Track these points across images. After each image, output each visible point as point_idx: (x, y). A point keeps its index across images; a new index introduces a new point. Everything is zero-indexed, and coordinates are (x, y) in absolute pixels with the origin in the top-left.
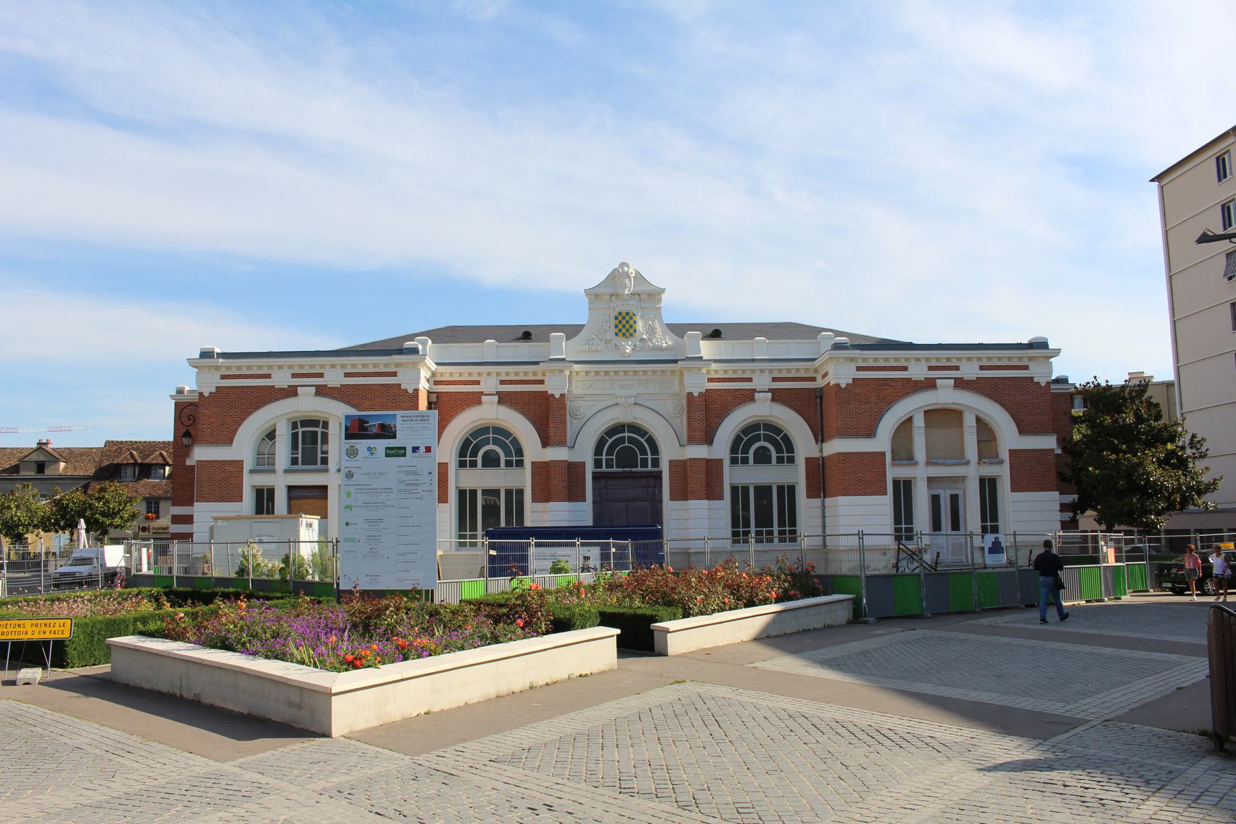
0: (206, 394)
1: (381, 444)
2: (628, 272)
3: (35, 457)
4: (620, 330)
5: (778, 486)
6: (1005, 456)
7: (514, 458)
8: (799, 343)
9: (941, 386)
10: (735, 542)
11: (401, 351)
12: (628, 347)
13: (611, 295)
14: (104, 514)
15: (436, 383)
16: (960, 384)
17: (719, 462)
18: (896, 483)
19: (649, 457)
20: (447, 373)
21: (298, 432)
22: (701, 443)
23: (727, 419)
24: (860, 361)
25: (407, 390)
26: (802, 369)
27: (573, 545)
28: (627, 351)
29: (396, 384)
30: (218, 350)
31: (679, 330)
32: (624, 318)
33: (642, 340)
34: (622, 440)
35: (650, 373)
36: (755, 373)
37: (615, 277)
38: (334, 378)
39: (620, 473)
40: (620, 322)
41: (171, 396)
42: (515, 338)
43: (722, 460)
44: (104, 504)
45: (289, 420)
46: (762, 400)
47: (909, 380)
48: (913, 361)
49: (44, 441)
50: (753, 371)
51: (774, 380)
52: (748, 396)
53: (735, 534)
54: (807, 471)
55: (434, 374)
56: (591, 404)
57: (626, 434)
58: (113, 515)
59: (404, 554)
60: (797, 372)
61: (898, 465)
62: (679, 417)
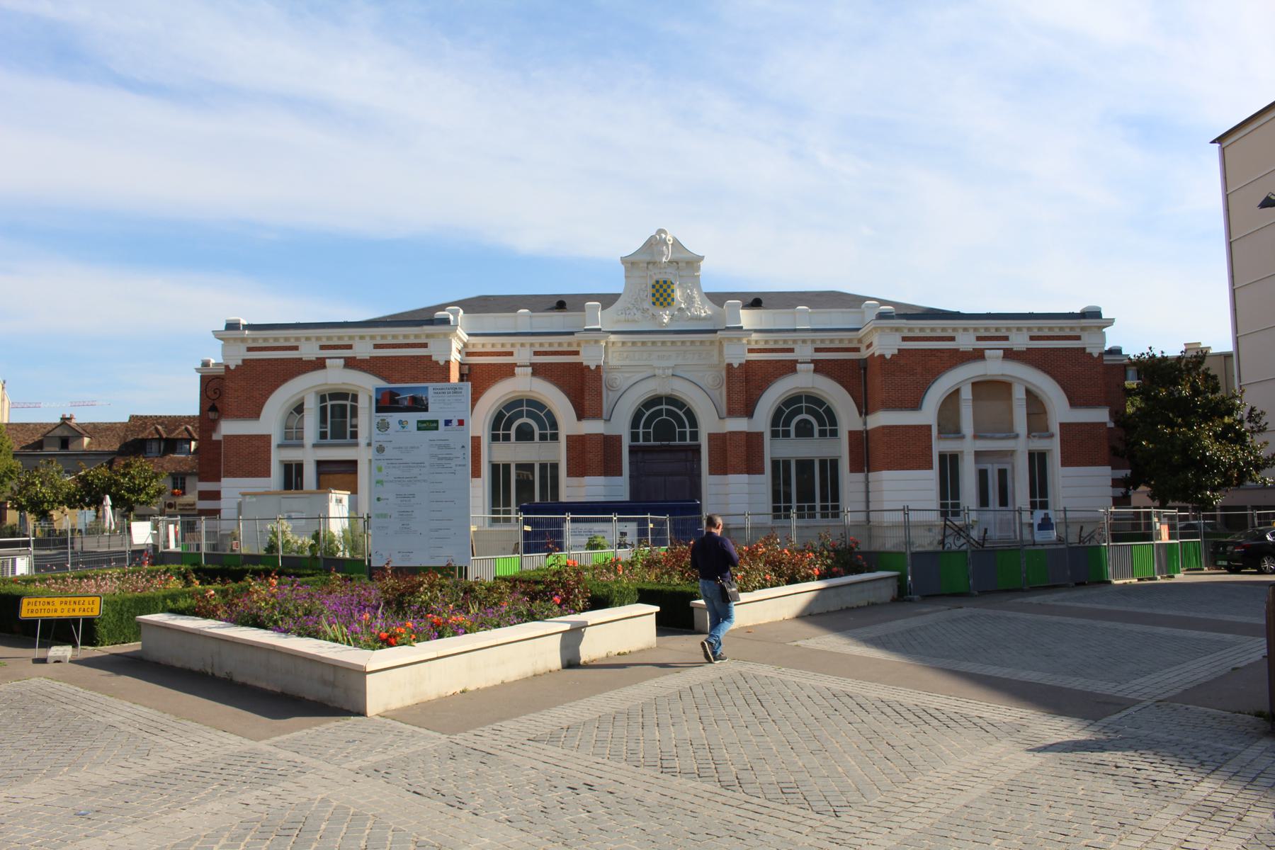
0: (232, 367)
1: (413, 418)
2: (665, 239)
3: (58, 432)
4: (658, 299)
6: (1055, 429)
7: (549, 432)
8: (842, 312)
9: (989, 358)
10: (776, 517)
11: (432, 322)
12: (666, 317)
13: (648, 263)
14: (129, 490)
15: (468, 354)
16: (1010, 355)
17: (760, 435)
18: (942, 457)
19: (688, 430)
20: (479, 343)
21: (326, 405)
22: (741, 416)
24: (906, 331)
27: (610, 520)
28: (665, 321)
30: (243, 322)
31: (718, 299)
32: (661, 286)
33: (680, 309)
34: (659, 412)
35: (688, 344)
37: (652, 244)
38: (363, 350)
39: (658, 446)
40: (658, 291)
41: (196, 369)
42: (549, 307)
44: (130, 480)
45: (317, 393)
47: (957, 350)
49: (68, 416)
50: (795, 341)
51: (817, 350)
52: (790, 368)
53: (776, 509)
54: (850, 444)
56: (627, 375)
57: (664, 407)
58: (139, 490)
59: (437, 530)
60: (840, 343)
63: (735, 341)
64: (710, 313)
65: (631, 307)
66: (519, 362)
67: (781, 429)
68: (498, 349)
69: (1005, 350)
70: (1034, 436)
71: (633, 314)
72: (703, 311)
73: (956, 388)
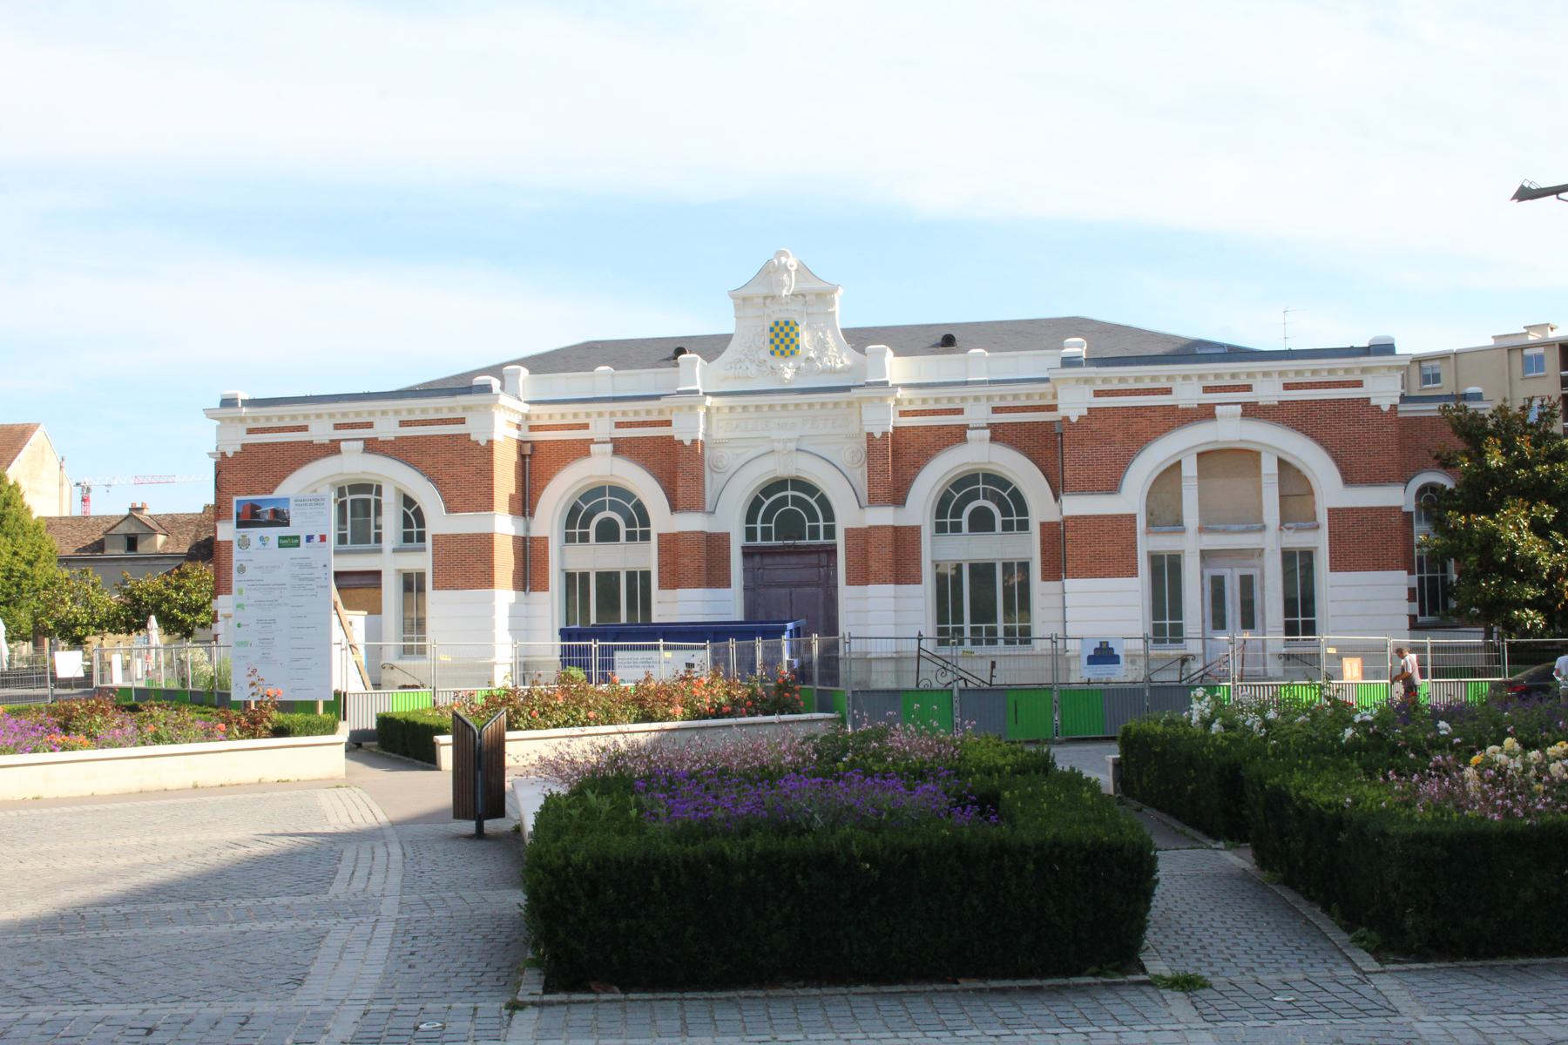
0: (230, 455)
1: (274, 533)
2: (786, 263)
3: (124, 529)
4: (777, 347)
6: (1323, 518)
7: (638, 529)
8: (1035, 355)
9: (1221, 416)
10: (942, 643)
11: (469, 390)
12: (788, 371)
13: (765, 298)
14: (183, 608)
15: (532, 428)
16: (1252, 411)
17: (916, 530)
18: (1156, 560)
19: (821, 524)
20: (544, 414)
21: (345, 501)
24: (1099, 382)
27: (656, 648)
29: (465, 435)
30: (243, 395)
31: (859, 338)
32: (782, 329)
33: (808, 359)
34: (783, 501)
37: (770, 272)
38: (387, 429)
39: (780, 547)
40: (777, 335)
41: (209, 454)
42: (666, 357)
44: (185, 594)
45: (333, 485)
47: (1174, 408)
49: (139, 505)
50: (963, 399)
52: (958, 435)
53: (941, 632)
54: (1043, 542)
55: (527, 417)
57: (789, 493)
58: (198, 610)
59: (298, 660)
60: (1040, 398)
61: (1158, 533)
67: (949, 520)
68: (570, 420)
69: (1244, 405)
70: (1289, 529)
72: (839, 361)
73: (1177, 459)
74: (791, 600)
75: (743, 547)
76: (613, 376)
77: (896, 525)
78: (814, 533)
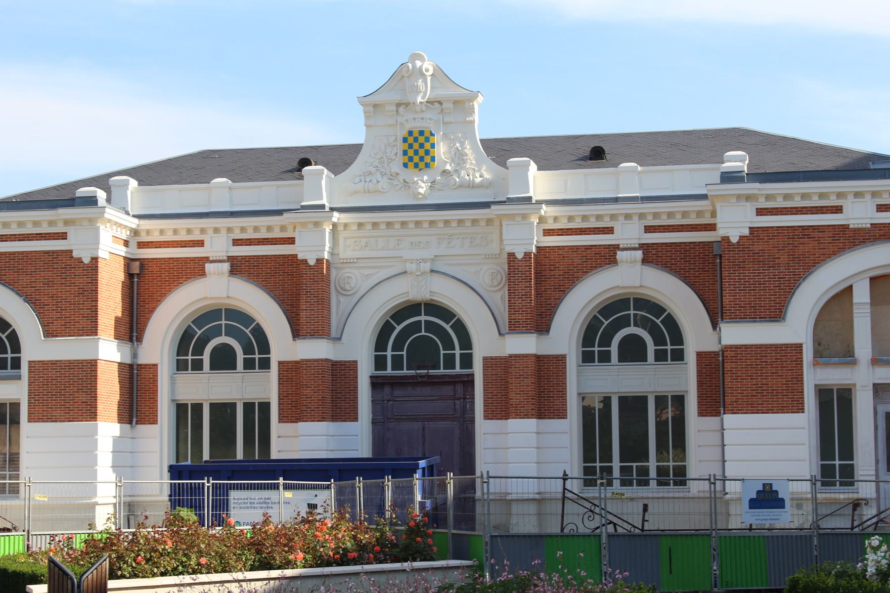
2: (421, 68)
4: (411, 159)
5: (620, 398)
8: (691, 170)
11: (72, 202)
12: (423, 185)
13: (398, 105)
15: (141, 245)
17: (560, 360)
18: (824, 394)
19: (458, 352)
20: (154, 229)
22: (528, 331)
23: (571, 294)
24: (762, 199)
25: (80, 258)
26: (678, 212)
27: (276, 487)
28: (421, 191)
29: (66, 251)
32: (416, 140)
35: (454, 224)
36: (617, 220)
37: (403, 76)
39: (412, 377)
40: (410, 146)
42: (290, 168)
43: (564, 357)
46: (627, 262)
47: (845, 227)
48: (851, 197)
50: (613, 217)
51: (649, 229)
53: (588, 471)
55: (135, 232)
56: (367, 272)
57: (423, 318)
61: (826, 364)
62: (500, 289)
63: (519, 219)
64: (488, 177)
65: (373, 170)
66: (212, 256)
68: (183, 237)
71: (374, 181)
72: (477, 175)
74: (424, 436)
75: (371, 377)
76: (230, 188)
77: (539, 353)
78: (450, 362)
